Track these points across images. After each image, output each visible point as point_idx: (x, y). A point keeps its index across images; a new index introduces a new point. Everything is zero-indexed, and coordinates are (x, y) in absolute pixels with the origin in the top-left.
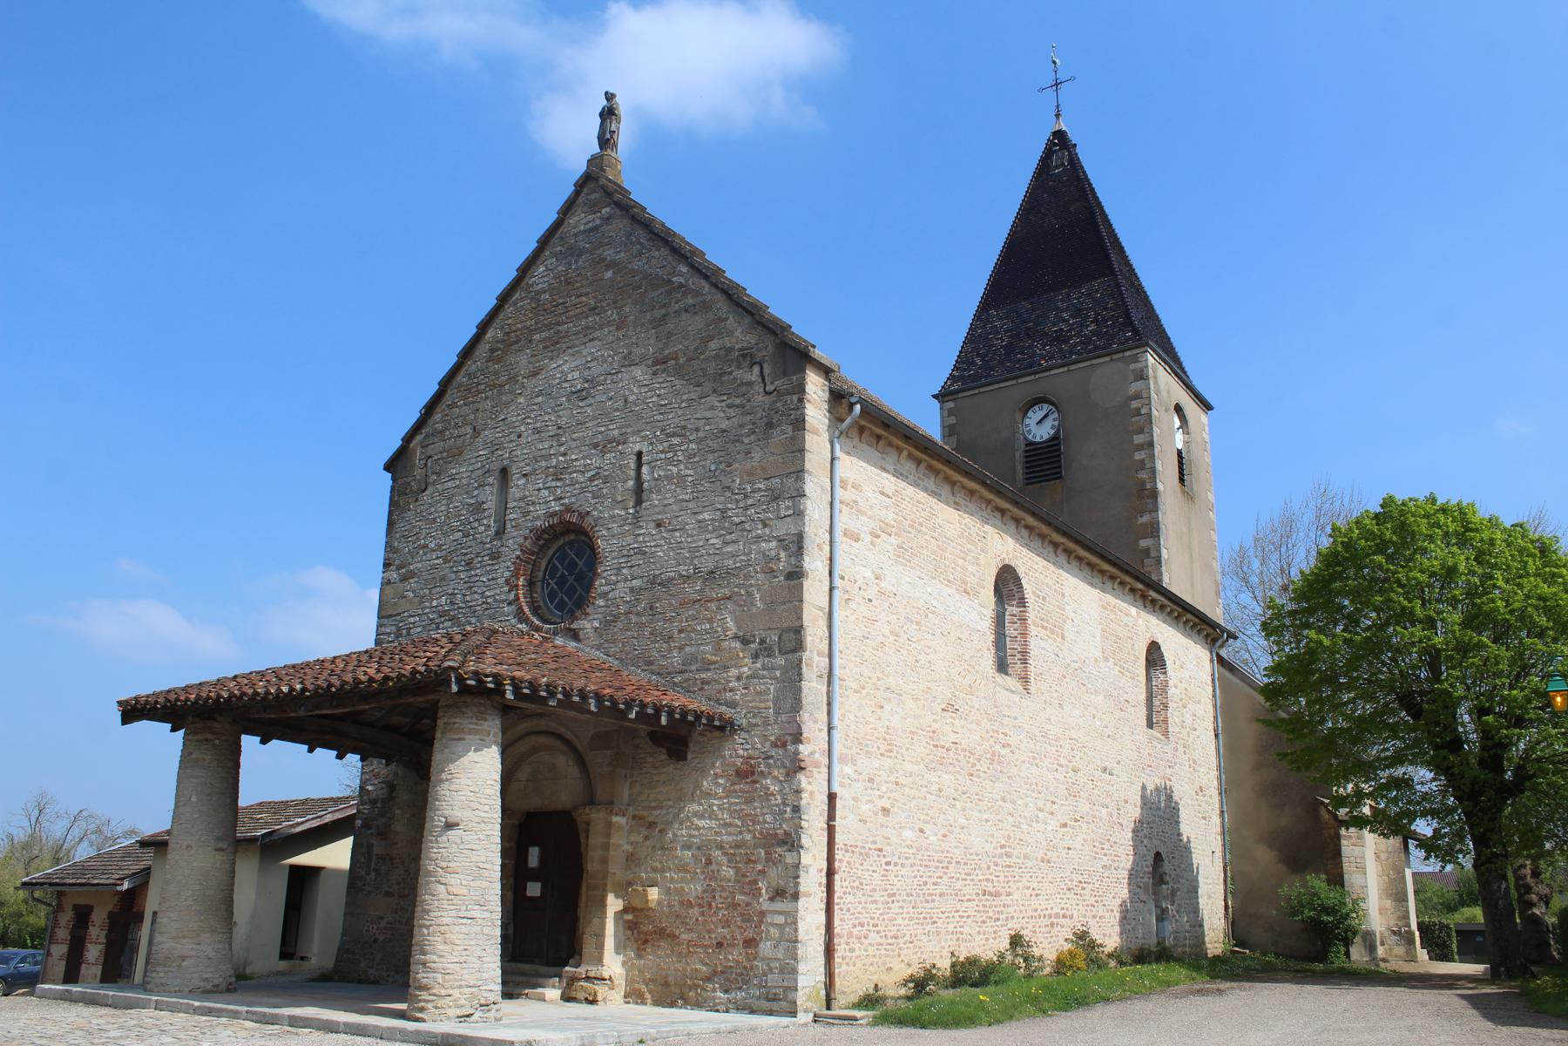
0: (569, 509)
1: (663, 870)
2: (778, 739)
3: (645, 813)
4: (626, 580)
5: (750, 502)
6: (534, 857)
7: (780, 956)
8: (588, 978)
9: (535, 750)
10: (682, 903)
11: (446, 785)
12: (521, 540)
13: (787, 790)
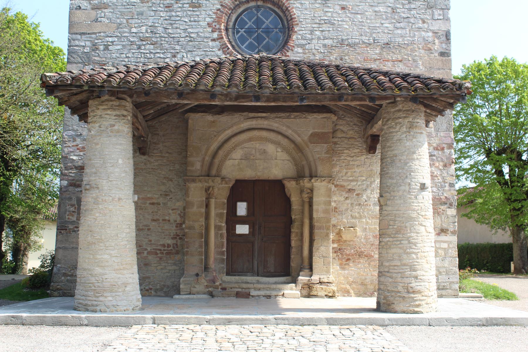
1: (361, 217)
2: (438, 145)
3: (345, 184)
4: (319, 39)
5: (413, 6)
6: (242, 209)
7: (446, 265)
8: (321, 283)
9: (267, 140)
11: (417, 162)
13: (446, 175)
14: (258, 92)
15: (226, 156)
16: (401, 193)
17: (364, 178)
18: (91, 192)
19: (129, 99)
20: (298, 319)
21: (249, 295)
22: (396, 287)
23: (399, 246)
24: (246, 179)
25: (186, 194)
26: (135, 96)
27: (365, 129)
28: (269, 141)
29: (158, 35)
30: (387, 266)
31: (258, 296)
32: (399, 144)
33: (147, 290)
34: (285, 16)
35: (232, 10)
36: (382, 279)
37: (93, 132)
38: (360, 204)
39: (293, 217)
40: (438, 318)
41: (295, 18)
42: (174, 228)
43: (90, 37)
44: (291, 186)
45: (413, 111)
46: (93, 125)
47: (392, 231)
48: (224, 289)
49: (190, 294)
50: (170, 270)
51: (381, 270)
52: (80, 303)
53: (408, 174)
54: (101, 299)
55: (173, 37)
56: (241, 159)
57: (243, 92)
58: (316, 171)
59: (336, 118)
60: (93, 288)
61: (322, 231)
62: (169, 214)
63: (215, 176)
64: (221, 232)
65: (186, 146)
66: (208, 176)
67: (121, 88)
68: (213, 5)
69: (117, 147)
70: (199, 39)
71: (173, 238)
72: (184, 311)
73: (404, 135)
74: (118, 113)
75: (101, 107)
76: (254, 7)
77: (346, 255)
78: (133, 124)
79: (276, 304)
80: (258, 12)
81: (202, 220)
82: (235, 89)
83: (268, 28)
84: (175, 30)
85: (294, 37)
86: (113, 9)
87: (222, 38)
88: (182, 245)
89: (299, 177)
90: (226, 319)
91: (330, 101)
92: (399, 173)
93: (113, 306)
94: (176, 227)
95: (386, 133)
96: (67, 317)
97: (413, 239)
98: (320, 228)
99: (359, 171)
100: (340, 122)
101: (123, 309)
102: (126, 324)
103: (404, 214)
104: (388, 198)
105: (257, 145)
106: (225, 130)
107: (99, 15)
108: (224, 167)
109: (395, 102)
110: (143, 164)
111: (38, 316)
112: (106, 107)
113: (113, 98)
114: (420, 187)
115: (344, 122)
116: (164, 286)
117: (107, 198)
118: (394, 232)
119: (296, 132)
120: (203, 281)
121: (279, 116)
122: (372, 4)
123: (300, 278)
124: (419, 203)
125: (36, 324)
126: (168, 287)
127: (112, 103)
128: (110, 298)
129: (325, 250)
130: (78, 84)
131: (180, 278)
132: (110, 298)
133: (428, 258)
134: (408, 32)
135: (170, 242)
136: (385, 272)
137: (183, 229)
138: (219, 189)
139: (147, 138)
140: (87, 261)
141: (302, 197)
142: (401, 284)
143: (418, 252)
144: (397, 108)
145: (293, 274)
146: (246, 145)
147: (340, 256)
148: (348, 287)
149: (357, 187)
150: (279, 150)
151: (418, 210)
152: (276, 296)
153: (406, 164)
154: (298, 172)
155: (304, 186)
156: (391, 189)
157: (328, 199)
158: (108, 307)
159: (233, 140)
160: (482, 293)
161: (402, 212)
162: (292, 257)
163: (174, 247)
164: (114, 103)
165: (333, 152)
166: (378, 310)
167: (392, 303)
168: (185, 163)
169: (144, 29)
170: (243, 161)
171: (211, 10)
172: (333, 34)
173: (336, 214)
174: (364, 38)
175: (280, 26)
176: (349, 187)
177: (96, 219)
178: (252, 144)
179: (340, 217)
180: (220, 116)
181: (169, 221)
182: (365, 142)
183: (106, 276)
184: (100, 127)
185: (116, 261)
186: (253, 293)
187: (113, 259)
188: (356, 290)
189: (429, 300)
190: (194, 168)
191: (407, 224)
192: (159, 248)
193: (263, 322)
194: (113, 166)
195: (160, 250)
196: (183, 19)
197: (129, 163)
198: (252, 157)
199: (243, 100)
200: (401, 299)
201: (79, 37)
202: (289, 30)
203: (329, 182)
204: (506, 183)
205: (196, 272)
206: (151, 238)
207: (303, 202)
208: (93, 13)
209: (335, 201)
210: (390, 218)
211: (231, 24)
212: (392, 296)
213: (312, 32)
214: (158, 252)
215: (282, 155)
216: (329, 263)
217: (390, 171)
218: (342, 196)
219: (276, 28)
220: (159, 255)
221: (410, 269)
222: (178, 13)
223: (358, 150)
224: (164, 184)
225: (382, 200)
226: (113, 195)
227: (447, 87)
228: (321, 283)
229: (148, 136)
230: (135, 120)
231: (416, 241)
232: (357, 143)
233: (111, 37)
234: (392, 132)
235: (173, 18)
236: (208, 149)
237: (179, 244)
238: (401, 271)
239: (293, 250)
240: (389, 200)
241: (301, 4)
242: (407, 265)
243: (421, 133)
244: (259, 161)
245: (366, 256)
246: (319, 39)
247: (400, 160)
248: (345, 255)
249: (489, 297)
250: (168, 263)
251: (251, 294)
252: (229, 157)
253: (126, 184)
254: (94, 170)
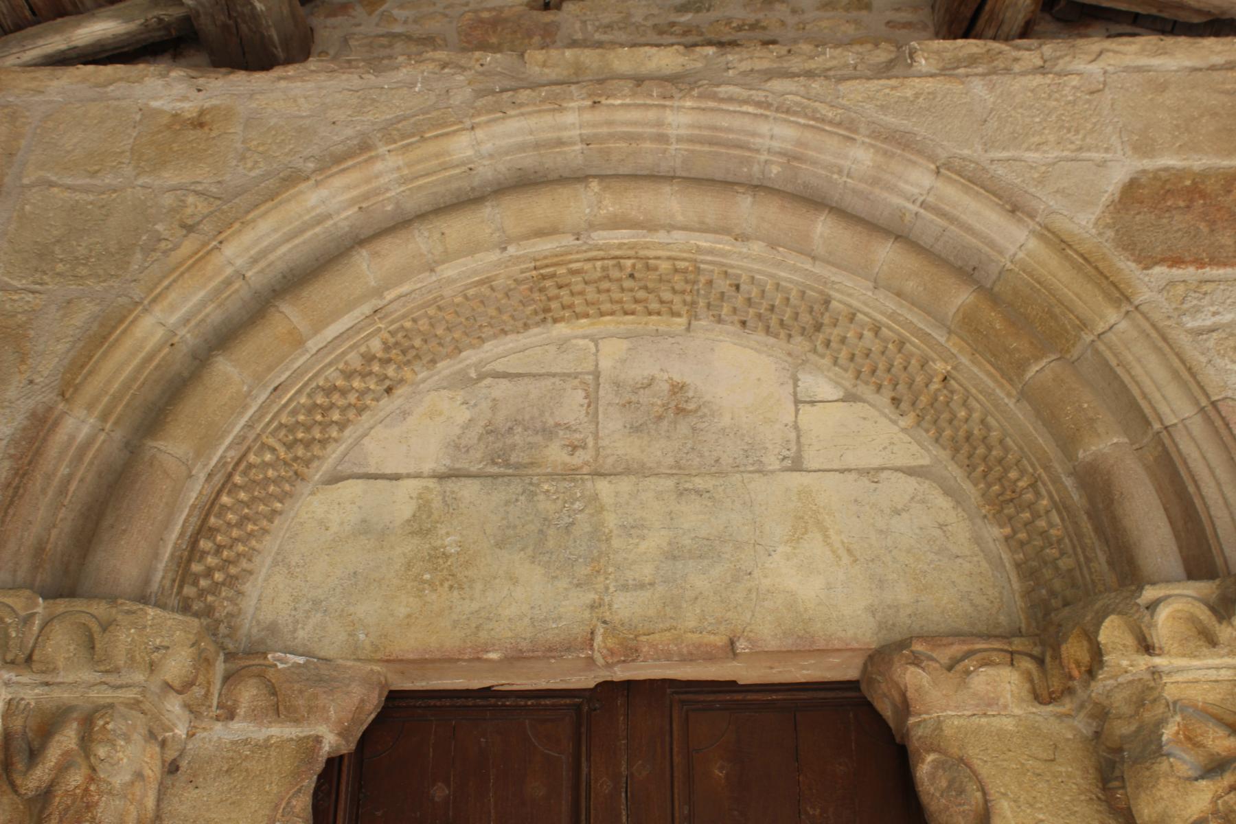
15: (307, 435)
56: (441, 477)
105: (611, 354)
108: (269, 545)
119: (976, 180)
146: (497, 351)
150: (820, 385)
154: (1029, 573)
155: (1146, 692)
170: (469, 490)
178: (562, 344)
198: (556, 454)
244: (625, 485)
252: (332, 456)
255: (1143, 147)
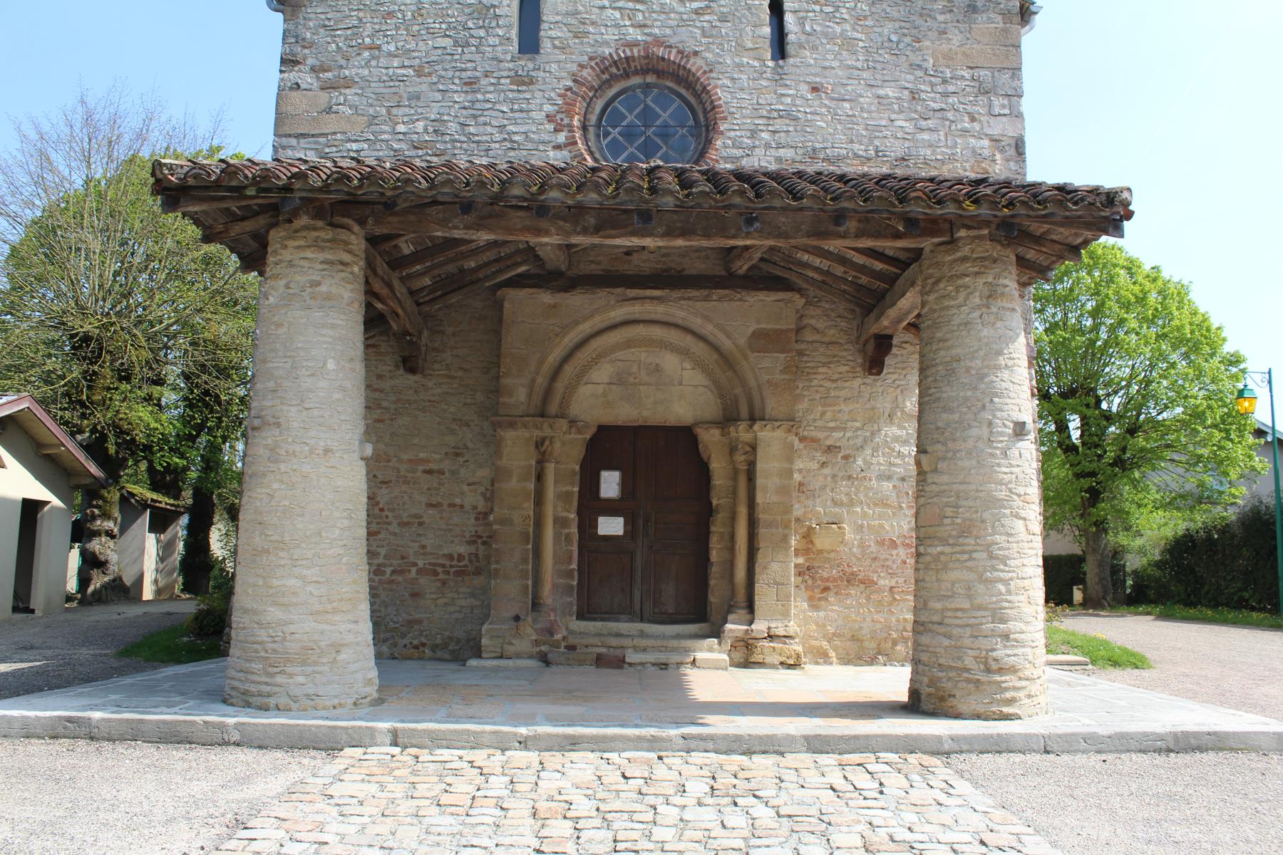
0: (659, 42)
1: (852, 503)
3: (821, 435)
5: (951, 88)
6: (610, 484)
8: (771, 637)
10: (881, 543)
11: (1005, 374)
12: (575, 68)
14: (647, 202)
16: (970, 443)
17: (858, 424)
18: (264, 434)
19: (356, 228)
20: (738, 739)
21: (623, 661)
22: (960, 658)
23: (968, 564)
24: (619, 423)
25: (498, 453)
26: (370, 221)
27: (861, 326)
28: (666, 348)
29: (448, 138)
30: (937, 611)
31: (642, 664)
32: (964, 333)
33: (416, 647)
34: (701, 102)
35: (596, 91)
36: (925, 639)
37: (271, 299)
38: (850, 477)
39: (715, 502)
40: (1066, 735)
41: (720, 106)
42: (473, 521)
43: (315, 143)
44: (710, 439)
45: (995, 261)
46: (273, 283)
47: (944, 528)
48: (571, 648)
49: (501, 657)
50: (462, 607)
51: (923, 618)
52: (233, 688)
53: (987, 400)
54: (279, 679)
55: (478, 142)
57: (612, 202)
58: (763, 408)
59: (804, 301)
60: (263, 654)
61: (774, 531)
62: (462, 493)
63: (556, 416)
64: (566, 531)
65: (499, 356)
66: (542, 416)
67: (330, 192)
68: (559, 79)
69: (324, 332)
70: (530, 146)
71: (468, 543)
72: (471, 710)
73: (976, 314)
74: (330, 257)
75: (291, 243)
76: (640, 86)
77: (822, 579)
78: (367, 282)
79: (680, 687)
80: (646, 97)
81: (529, 507)
82: (594, 196)
83: (666, 126)
84: (481, 129)
85: (719, 143)
86: (362, 88)
87: (576, 143)
88: (488, 558)
89: (727, 419)
90: (566, 737)
91: (809, 236)
92: (966, 399)
93: (308, 696)
94: (477, 519)
95: (935, 311)
96: (193, 723)
97: (999, 549)
98: (770, 525)
99: (847, 410)
100: (812, 311)
101: (328, 703)
102: (329, 745)
103: (978, 491)
104: (940, 455)
105: (643, 356)
106: (577, 323)
107: (334, 101)
109: (953, 241)
110: (411, 392)
111: (127, 720)
112: (302, 243)
113: (320, 224)
114: (1014, 430)
115: (819, 312)
116: (451, 638)
117: (297, 448)
118: (954, 533)
120: (529, 630)
121: (687, 295)
122: (872, 83)
123: (729, 626)
124: (1011, 466)
125: (123, 739)
126: (458, 641)
127: (316, 234)
128: (301, 679)
129: (779, 570)
130: (234, 183)
131: (483, 624)
132: (301, 679)
133: (1031, 593)
134: (942, 138)
135: (463, 549)
136: (933, 623)
137: (489, 524)
138: (563, 444)
139: (419, 337)
140: (250, 591)
141: (732, 462)
142: (971, 652)
143: (1011, 579)
144: (959, 254)
145: (712, 618)
146: (620, 354)
147: (810, 582)
148: (825, 644)
149: (845, 441)
150: (687, 365)
151: (1010, 482)
152: (679, 664)
153: (981, 377)
154: (724, 410)
155: (737, 439)
156: (947, 434)
157: (786, 465)
158: (295, 699)
159: (596, 344)
160: (1084, 654)
161: (973, 487)
162: (712, 582)
163: (470, 561)
164: (322, 234)
165: (796, 370)
166: (915, 706)
167: (950, 696)
168: (495, 390)
169: (420, 126)
170: (614, 387)
171: (553, 89)
172: (797, 138)
173: (803, 498)
174: (856, 146)
175: (691, 122)
176: (828, 443)
177: (272, 496)
179: (810, 503)
180: (567, 295)
181: (462, 507)
182: (863, 351)
183: (292, 628)
184: (287, 286)
185: (316, 593)
186: (632, 657)
187: (310, 588)
188: (840, 651)
189: (1034, 688)
190: (513, 400)
191: (986, 515)
192: (440, 561)
193: (652, 744)
194: (312, 375)
195: (443, 566)
196: (497, 107)
197: (353, 370)
198: (631, 380)
199: (613, 232)
200: (971, 686)
201: (293, 142)
202: (707, 130)
203: (789, 431)
204: (1073, 448)
205: (512, 614)
206: (425, 542)
207: (736, 472)
208: (324, 96)
209: (800, 471)
210: (945, 500)
211: (593, 118)
212: (949, 679)
213: (753, 134)
214: (440, 570)
215: (693, 377)
216: (788, 597)
217: (945, 395)
218: (813, 459)
219: (683, 127)
220: (442, 576)
221: (993, 617)
222: (489, 96)
223: (847, 368)
224: (452, 432)
225: (924, 459)
226: (312, 441)
227: (1082, 200)
228: (771, 637)
229: (420, 333)
230: (369, 272)
231: (1006, 553)
232: (845, 354)
233: (356, 141)
234: (947, 308)
235: (478, 106)
236: (542, 362)
237: (481, 553)
238: (972, 621)
239: (715, 570)
240: (944, 459)
241: (733, 79)
242: (986, 609)
243: (1013, 310)
245: (862, 582)
246: (767, 146)
247: (968, 370)
248: (821, 581)
249: (1100, 662)
250: (459, 593)
251: (627, 660)
253: (343, 418)
254: (271, 384)
255: (758, 322)
